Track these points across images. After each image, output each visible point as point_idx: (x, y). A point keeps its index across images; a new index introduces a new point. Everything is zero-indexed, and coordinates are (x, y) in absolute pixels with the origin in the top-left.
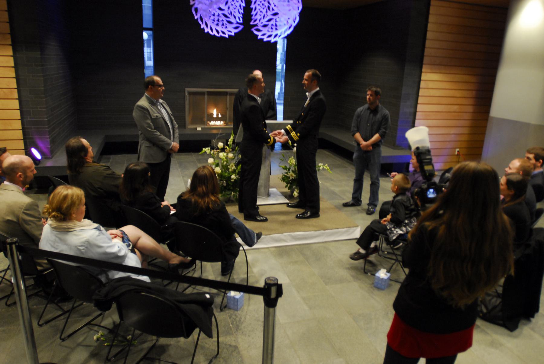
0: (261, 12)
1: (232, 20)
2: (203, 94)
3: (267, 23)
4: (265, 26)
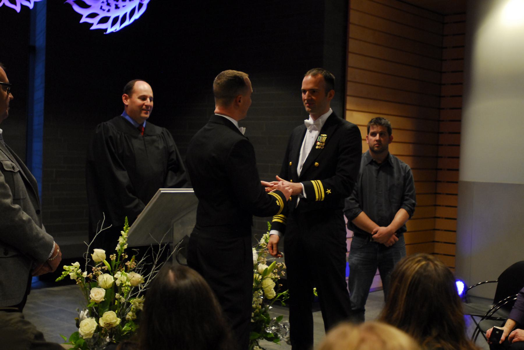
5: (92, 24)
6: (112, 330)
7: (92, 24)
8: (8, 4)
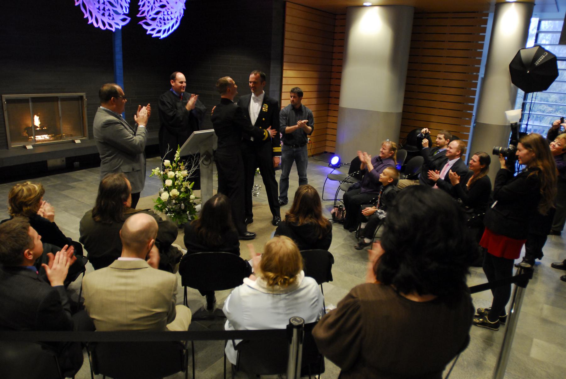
0: (149, 2)
1: (119, 10)
2: (26, 101)
3: (155, 16)
4: (154, 19)
5: (153, 34)
6: (177, 198)
7: (153, 34)
8: (109, 28)
